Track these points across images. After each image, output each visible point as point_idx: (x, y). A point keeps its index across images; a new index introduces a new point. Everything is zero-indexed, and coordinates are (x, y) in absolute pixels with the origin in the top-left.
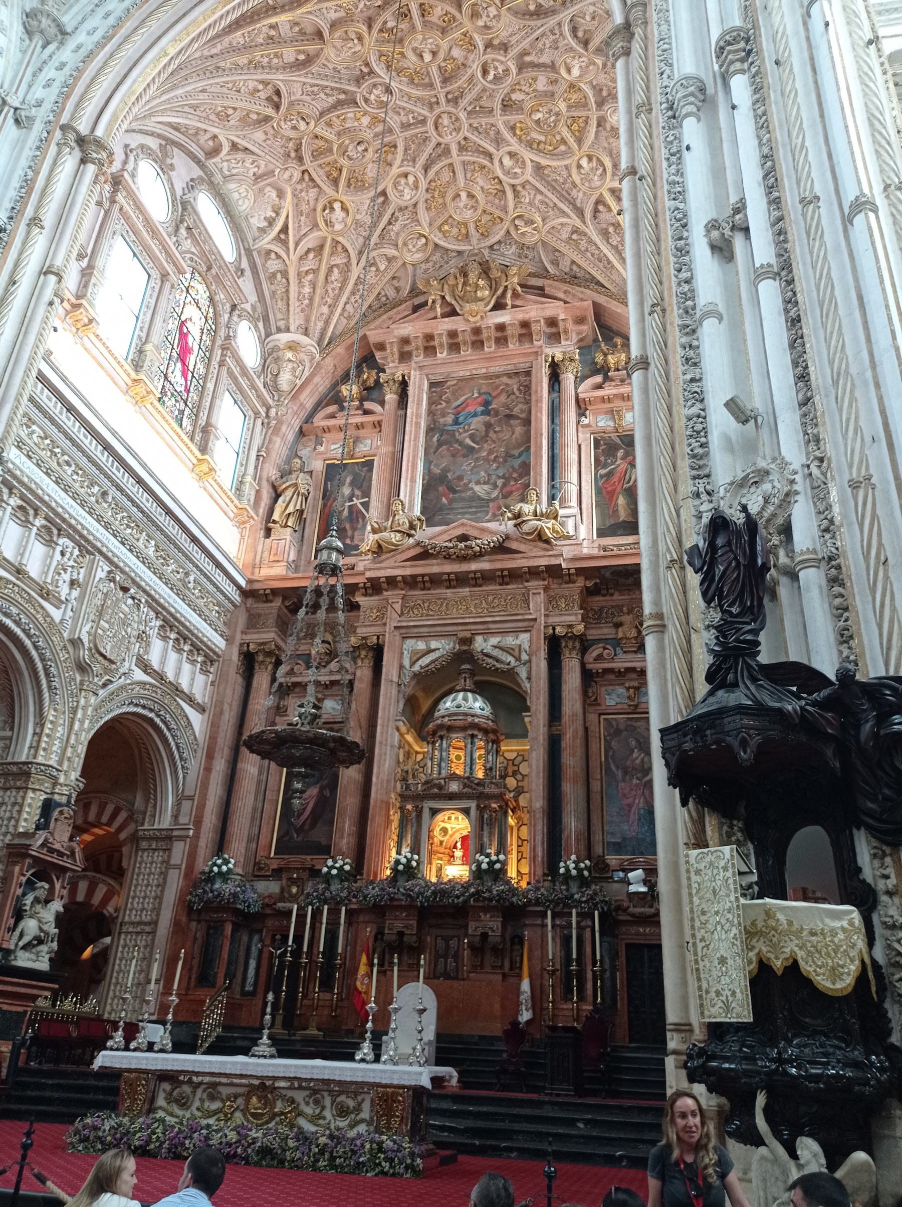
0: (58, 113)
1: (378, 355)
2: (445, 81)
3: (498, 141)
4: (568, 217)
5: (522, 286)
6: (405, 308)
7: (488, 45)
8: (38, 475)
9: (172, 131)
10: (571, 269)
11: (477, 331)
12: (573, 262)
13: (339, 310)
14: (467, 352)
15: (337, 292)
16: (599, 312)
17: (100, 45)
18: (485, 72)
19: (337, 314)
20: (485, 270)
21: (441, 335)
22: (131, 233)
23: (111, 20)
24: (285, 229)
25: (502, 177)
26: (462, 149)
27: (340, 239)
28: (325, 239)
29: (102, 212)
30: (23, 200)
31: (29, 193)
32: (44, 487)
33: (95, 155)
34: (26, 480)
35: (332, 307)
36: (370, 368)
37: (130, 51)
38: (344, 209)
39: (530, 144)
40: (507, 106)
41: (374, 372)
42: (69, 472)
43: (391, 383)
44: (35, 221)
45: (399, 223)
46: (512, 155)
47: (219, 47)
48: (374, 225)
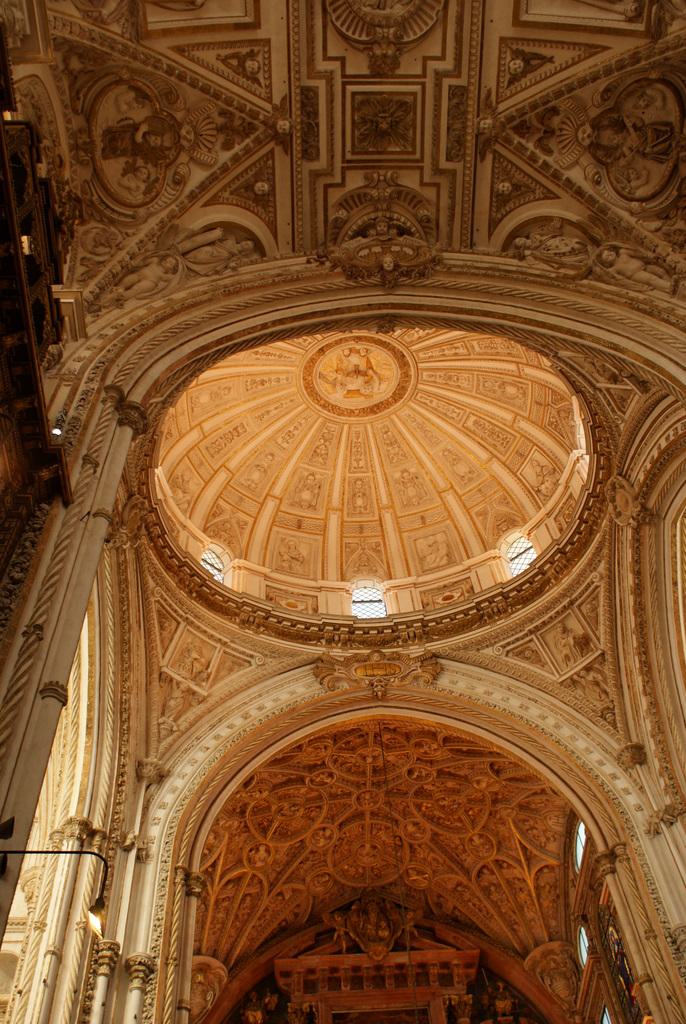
1: (281, 982)
2: (375, 771)
3: (405, 813)
4: (457, 873)
5: (416, 926)
6: (306, 937)
7: (418, 759)
10: (453, 913)
11: (378, 968)
12: (455, 908)
13: (246, 934)
14: (368, 988)
15: (246, 917)
16: (483, 955)
18: (410, 772)
19: (244, 939)
20: (383, 911)
21: (345, 969)
24: (214, 865)
25: (404, 837)
26: (373, 814)
27: (260, 875)
28: (245, 873)
35: (240, 932)
36: (272, 993)
38: (268, 851)
39: (431, 819)
40: (420, 793)
41: (275, 998)
43: (299, 1014)
45: (309, 863)
46: (415, 824)
48: (288, 864)
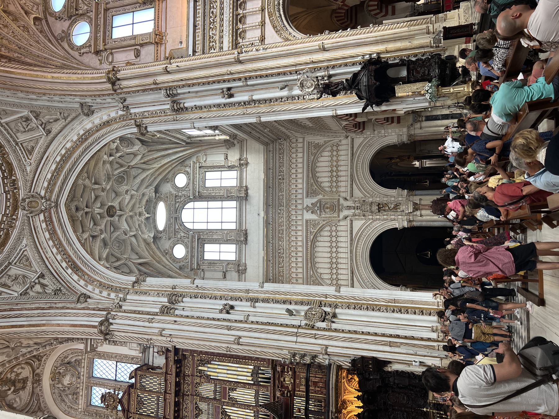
0: (112, 94)
8: (226, 24)
9: (53, 42)
17: (75, 95)
22: (107, 35)
23: (62, 97)
29: (113, 51)
30: (151, 89)
31: (148, 89)
32: (228, 18)
33: (114, 78)
34: (231, 27)
37: (65, 87)
42: (215, 10)
44: (155, 83)
47: (16, 55)
